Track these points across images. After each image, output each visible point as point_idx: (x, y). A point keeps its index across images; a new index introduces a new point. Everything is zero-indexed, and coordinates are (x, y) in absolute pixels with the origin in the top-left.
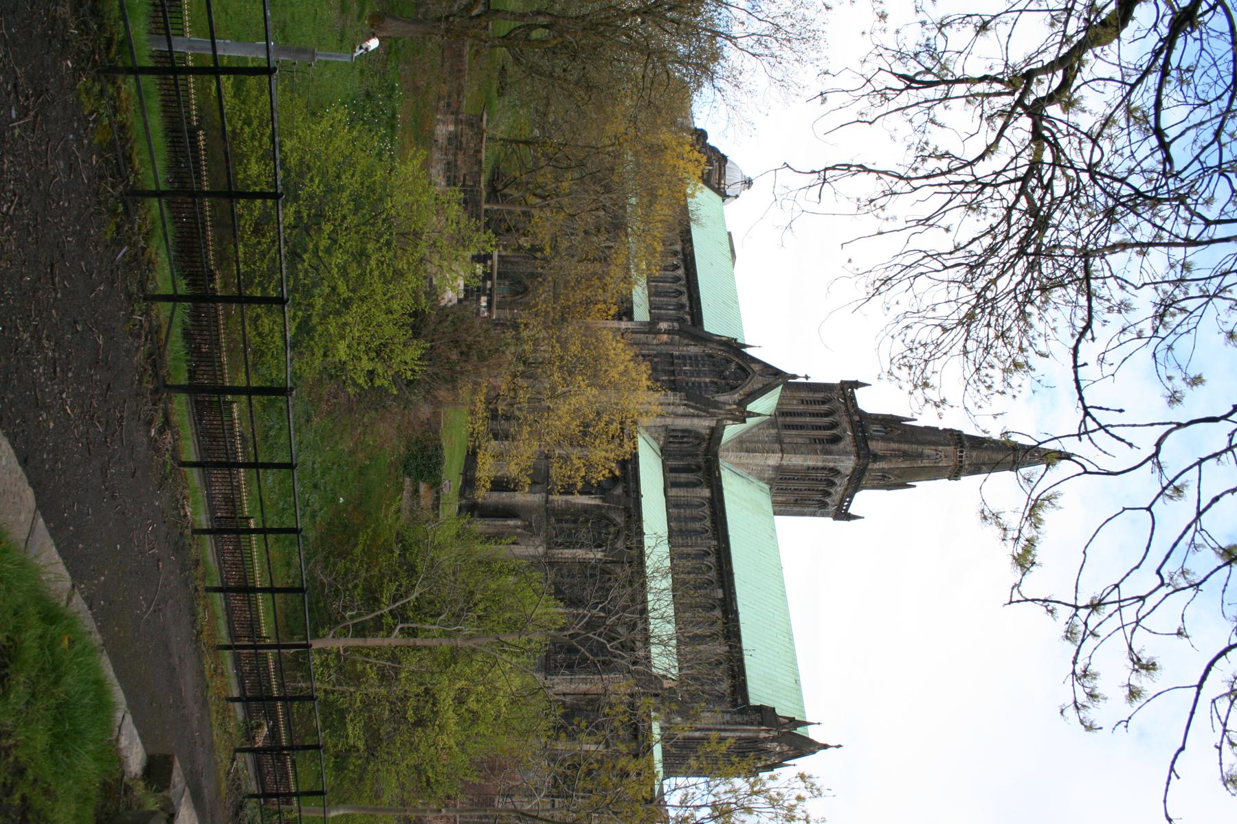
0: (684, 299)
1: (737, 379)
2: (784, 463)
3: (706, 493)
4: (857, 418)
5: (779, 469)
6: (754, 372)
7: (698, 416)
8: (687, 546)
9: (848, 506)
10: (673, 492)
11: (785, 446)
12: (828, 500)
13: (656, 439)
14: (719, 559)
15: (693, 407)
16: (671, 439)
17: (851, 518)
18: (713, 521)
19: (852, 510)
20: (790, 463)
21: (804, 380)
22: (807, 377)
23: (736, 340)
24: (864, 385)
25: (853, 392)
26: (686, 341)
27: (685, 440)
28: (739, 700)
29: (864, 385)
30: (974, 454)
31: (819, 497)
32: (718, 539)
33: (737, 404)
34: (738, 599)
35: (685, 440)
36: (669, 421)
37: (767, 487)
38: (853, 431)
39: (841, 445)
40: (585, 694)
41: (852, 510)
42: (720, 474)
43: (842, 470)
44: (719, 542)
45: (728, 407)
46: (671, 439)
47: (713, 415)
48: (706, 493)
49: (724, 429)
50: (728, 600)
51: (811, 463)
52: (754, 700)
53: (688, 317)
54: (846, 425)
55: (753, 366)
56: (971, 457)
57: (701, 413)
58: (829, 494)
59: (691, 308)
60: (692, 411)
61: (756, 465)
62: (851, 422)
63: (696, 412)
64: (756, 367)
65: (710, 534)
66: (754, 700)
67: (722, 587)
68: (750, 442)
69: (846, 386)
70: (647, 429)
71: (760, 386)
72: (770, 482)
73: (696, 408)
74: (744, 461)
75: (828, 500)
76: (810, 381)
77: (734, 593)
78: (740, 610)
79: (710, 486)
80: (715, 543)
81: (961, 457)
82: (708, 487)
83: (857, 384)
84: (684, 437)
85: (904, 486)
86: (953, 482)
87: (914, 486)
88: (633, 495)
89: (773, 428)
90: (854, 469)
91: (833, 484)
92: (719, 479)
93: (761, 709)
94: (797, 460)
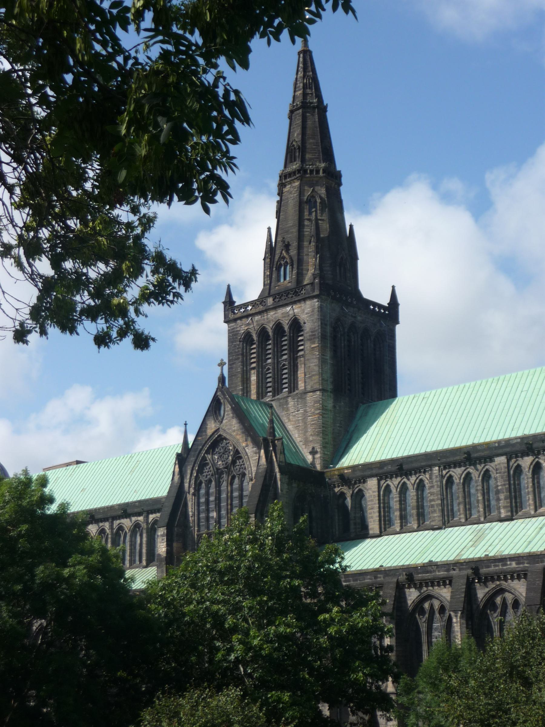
0: (127, 523)
1: (226, 451)
2: (330, 387)
3: (372, 484)
4: (270, 301)
6: (217, 430)
9: (380, 306)
10: (374, 526)
11: (309, 388)
14: (457, 464)
18: (408, 474)
19: (385, 301)
20: (331, 380)
21: (226, 368)
22: (221, 364)
23: (178, 456)
24: (229, 294)
25: (240, 306)
29: (229, 294)
30: (308, 156)
32: (431, 466)
33: (260, 449)
34: (507, 436)
37: (362, 407)
38: (286, 305)
41: (385, 301)
42: (348, 468)
44: (435, 465)
45: (263, 460)
49: (290, 464)
50: (508, 450)
53: (151, 517)
54: (281, 311)
55: (209, 432)
56: (310, 159)
59: (139, 514)
62: (275, 308)
64: (212, 426)
65: (425, 477)
67: (490, 459)
68: (306, 432)
69: (231, 316)
71: (234, 421)
76: (226, 360)
77: (499, 442)
78: (520, 434)
79: (363, 480)
80: (436, 469)
81: (312, 171)
82: (364, 482)
83: (229, 303)
85: (352, 237)
86: (343, 180)
87: (351, 227)
88: (381, 578)
89: (287, 403)
92: (354, 468)
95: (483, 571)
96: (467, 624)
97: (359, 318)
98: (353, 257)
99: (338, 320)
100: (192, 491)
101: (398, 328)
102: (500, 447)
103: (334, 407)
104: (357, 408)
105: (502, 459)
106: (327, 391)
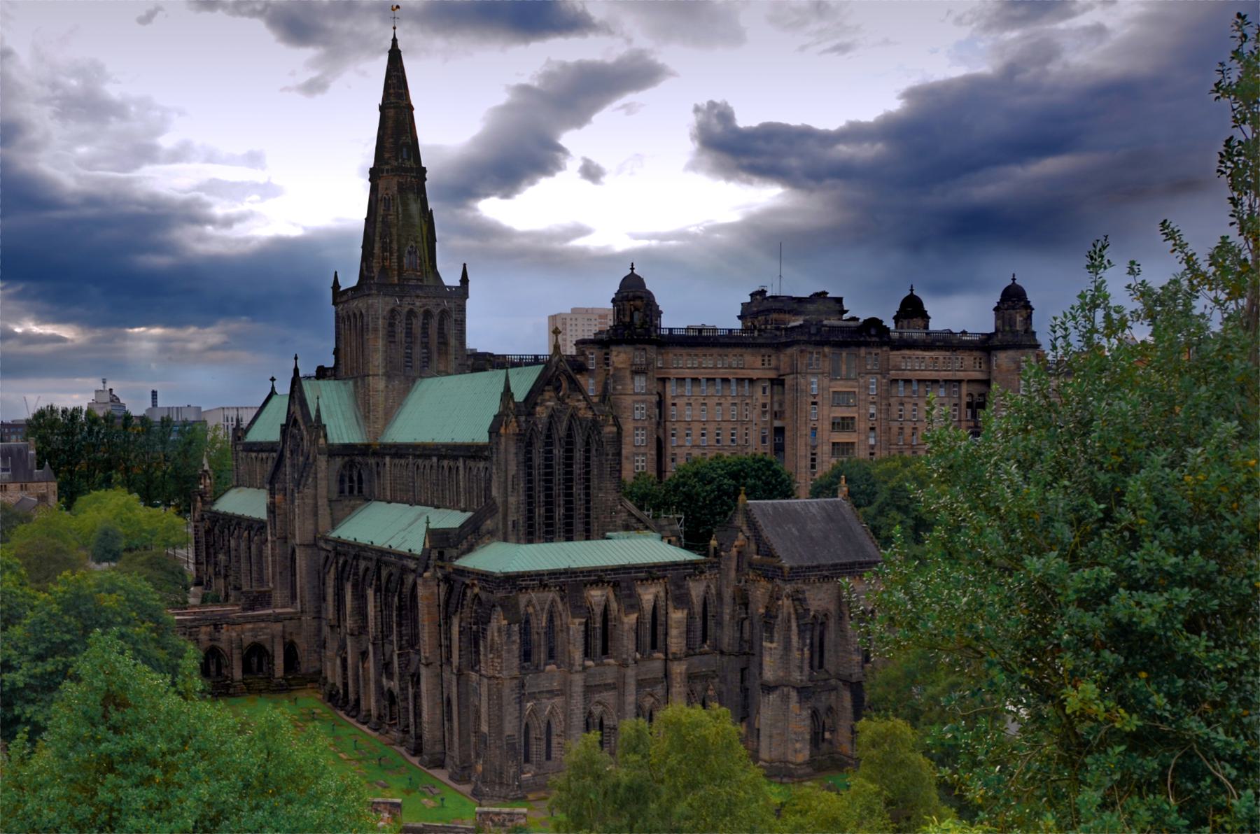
3: (388, 459)
5: (389, 376)
7: (316, 474)
8: (414, 487)
12: (436, 311)
13: (353, 509)
14: (419, 456)
15: (307, 480)
16: (356, 492)
17: (465, 280)
23: (282, 426)
26: (282, 477)
27: (355, 478)
28: (486, 453)
31: (434, 323)
35: (355, 478)
36: (322, 502)
37: (419, 380)
39: (363, 311)
40: (440, 626)
43: (388, 308)
46: (356, 492)
47: (315, 460)
48: (388, 459)
49: (332, 445)
51: (380, 344)
52: (487, 440)
57: (313, 471)
58: (427, 314)
60: (310, 480)
61: (386, 399)
63: (312, 475)
66: (482, 437)
70: (334, 524)
72: (410, 382)
73: (308, 476)
74: (381, 413)
75: (436, 311)
79: (383, 456)
83: (336, 285)
84: (351, 480)
90: (385, 295)
91: (411, 313)
92: (380, 445)
93: (490, 433)
94: (377, 360)
95: (386, 558)
96: (375, 595)
97: (418, 304)
98: (434, 240)
99: (393, 310)
100: (288, 455)
101: (468, 301)
102: (434, 450)
103: (387, 387)
104: (414, 381)
105: (435, 459)
106: (378, 375)
